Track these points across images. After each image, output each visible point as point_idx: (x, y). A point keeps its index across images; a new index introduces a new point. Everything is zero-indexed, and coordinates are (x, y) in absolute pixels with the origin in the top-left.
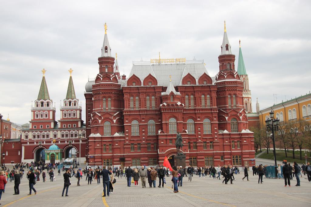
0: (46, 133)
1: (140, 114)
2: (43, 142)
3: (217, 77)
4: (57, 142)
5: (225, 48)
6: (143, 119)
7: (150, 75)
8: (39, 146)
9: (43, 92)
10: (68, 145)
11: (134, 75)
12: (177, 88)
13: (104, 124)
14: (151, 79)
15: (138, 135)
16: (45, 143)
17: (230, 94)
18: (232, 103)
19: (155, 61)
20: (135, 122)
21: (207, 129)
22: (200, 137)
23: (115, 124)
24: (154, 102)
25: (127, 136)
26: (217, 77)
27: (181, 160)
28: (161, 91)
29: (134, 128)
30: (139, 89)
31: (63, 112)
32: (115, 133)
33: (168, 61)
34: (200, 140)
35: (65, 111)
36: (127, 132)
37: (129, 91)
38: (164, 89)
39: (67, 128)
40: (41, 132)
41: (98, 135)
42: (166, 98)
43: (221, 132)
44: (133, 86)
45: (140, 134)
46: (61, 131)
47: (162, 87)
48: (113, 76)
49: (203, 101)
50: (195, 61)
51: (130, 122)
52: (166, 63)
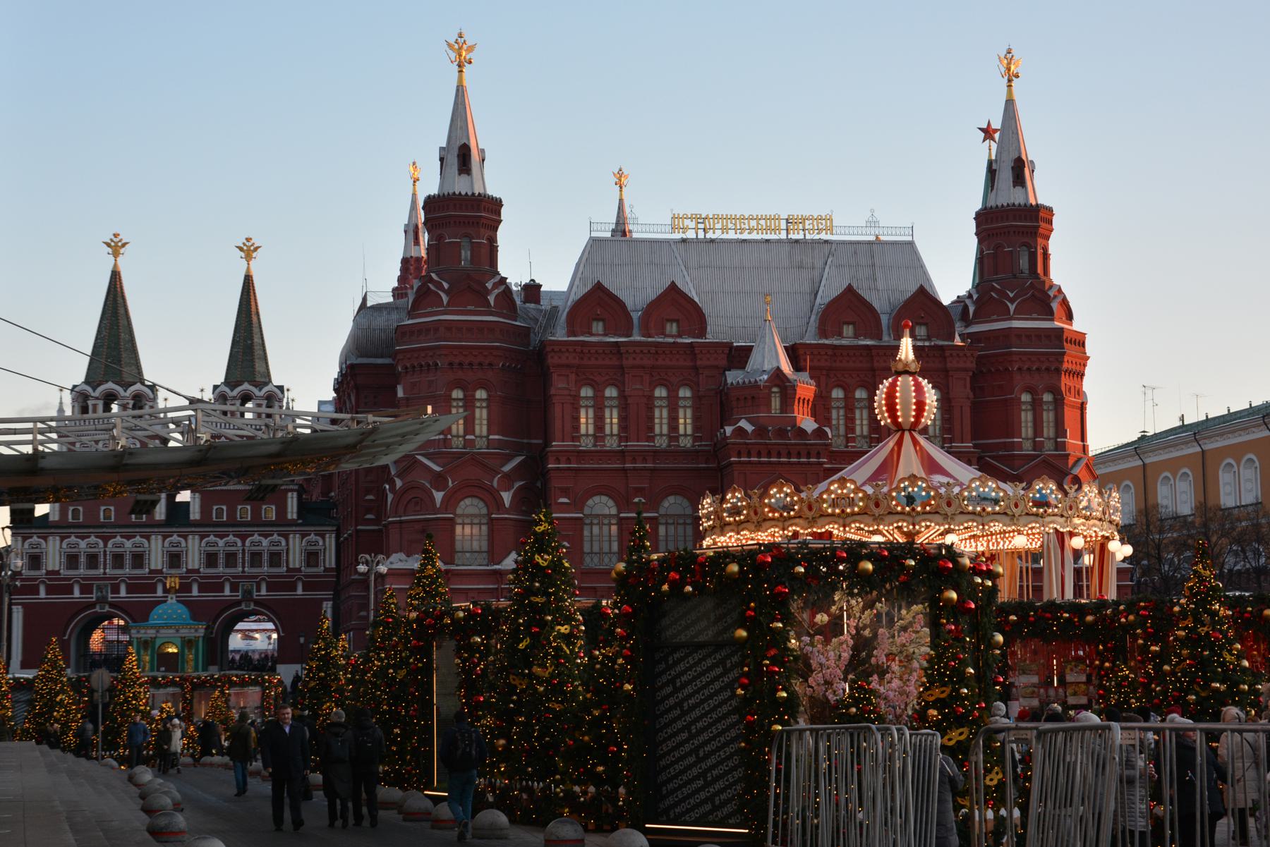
1: (624, 470)
2: (116, 590)
3: (972, 309)
4: (185, 588)
5: (1005, 176)
6: (639, 491)
7: (673, 286)
8: (93, 605)
10: (238, 603)
11: (599, 287)
12: (794, 353)
13: (459, 511)
14: (675, 305)
16: (123, 593)
17: (1030, 390)
18: (1038, 430)
23: (507, 511)
26: (972, 309)
29: (596, 530)
30: (623, 349)
33: (753, 223)
38: (739, 356)
39: (233, 523)
40: (106, 539)
42: (753, 396)
44: (591, 335)
46: (202, 538)
47: (729, 346)
48: (495, 286)
52: (746, 236)
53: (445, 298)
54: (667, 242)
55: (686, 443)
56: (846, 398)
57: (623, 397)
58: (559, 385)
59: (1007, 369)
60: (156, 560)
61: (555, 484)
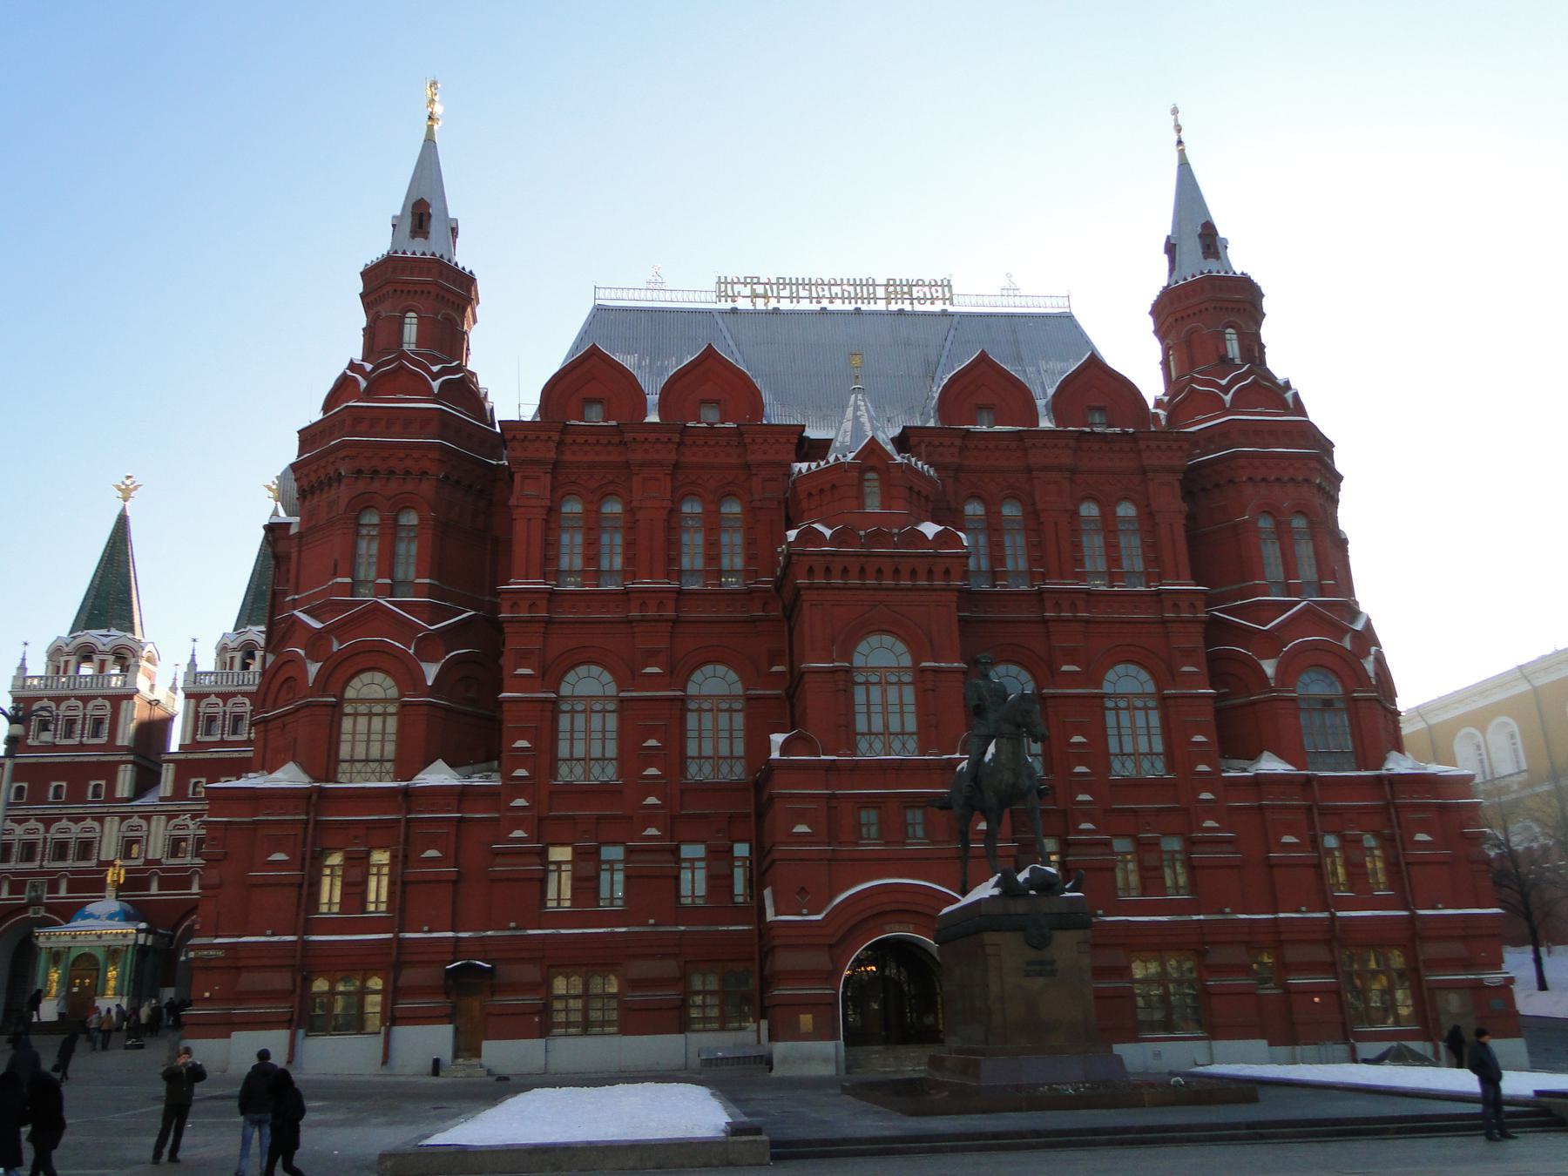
0: (75, 829)
2: (53, 887)
6: (650, 657)
7: (710, 353)
8: (24, 908)
9: (110, 597)
11: (594, 352)
15: (607, 773)
16: (63, 892)
19: (747, 291)
20: (589, 682)
21: (1136, 741)
22: (1086, 797)
24: (738, 539)
25: (518, 787)
27: (1041, 943)
28: (793, 456)
29: (580, 720)
31: (198, 706)
32: (427, 762)
33: (835, 290)
34: (1089, 826)
35: (213, 699)
36: (521, 758)
37: (552, 455)
40: (48, 822)
41: (289, 777)
43: (1234, 771)
45: (621, 772)
49: (1093, 545)
50: (1017, 301)
51: (551, 674)
53: (363, 384)
54: (710, 312)
55: (732, 583)
56: (988, 513)
57: (630, 510)
58: (529, 492)
59: (1231, 481)
60: (109, 848)
61: (513, 643)
